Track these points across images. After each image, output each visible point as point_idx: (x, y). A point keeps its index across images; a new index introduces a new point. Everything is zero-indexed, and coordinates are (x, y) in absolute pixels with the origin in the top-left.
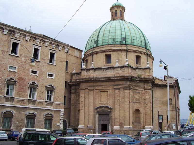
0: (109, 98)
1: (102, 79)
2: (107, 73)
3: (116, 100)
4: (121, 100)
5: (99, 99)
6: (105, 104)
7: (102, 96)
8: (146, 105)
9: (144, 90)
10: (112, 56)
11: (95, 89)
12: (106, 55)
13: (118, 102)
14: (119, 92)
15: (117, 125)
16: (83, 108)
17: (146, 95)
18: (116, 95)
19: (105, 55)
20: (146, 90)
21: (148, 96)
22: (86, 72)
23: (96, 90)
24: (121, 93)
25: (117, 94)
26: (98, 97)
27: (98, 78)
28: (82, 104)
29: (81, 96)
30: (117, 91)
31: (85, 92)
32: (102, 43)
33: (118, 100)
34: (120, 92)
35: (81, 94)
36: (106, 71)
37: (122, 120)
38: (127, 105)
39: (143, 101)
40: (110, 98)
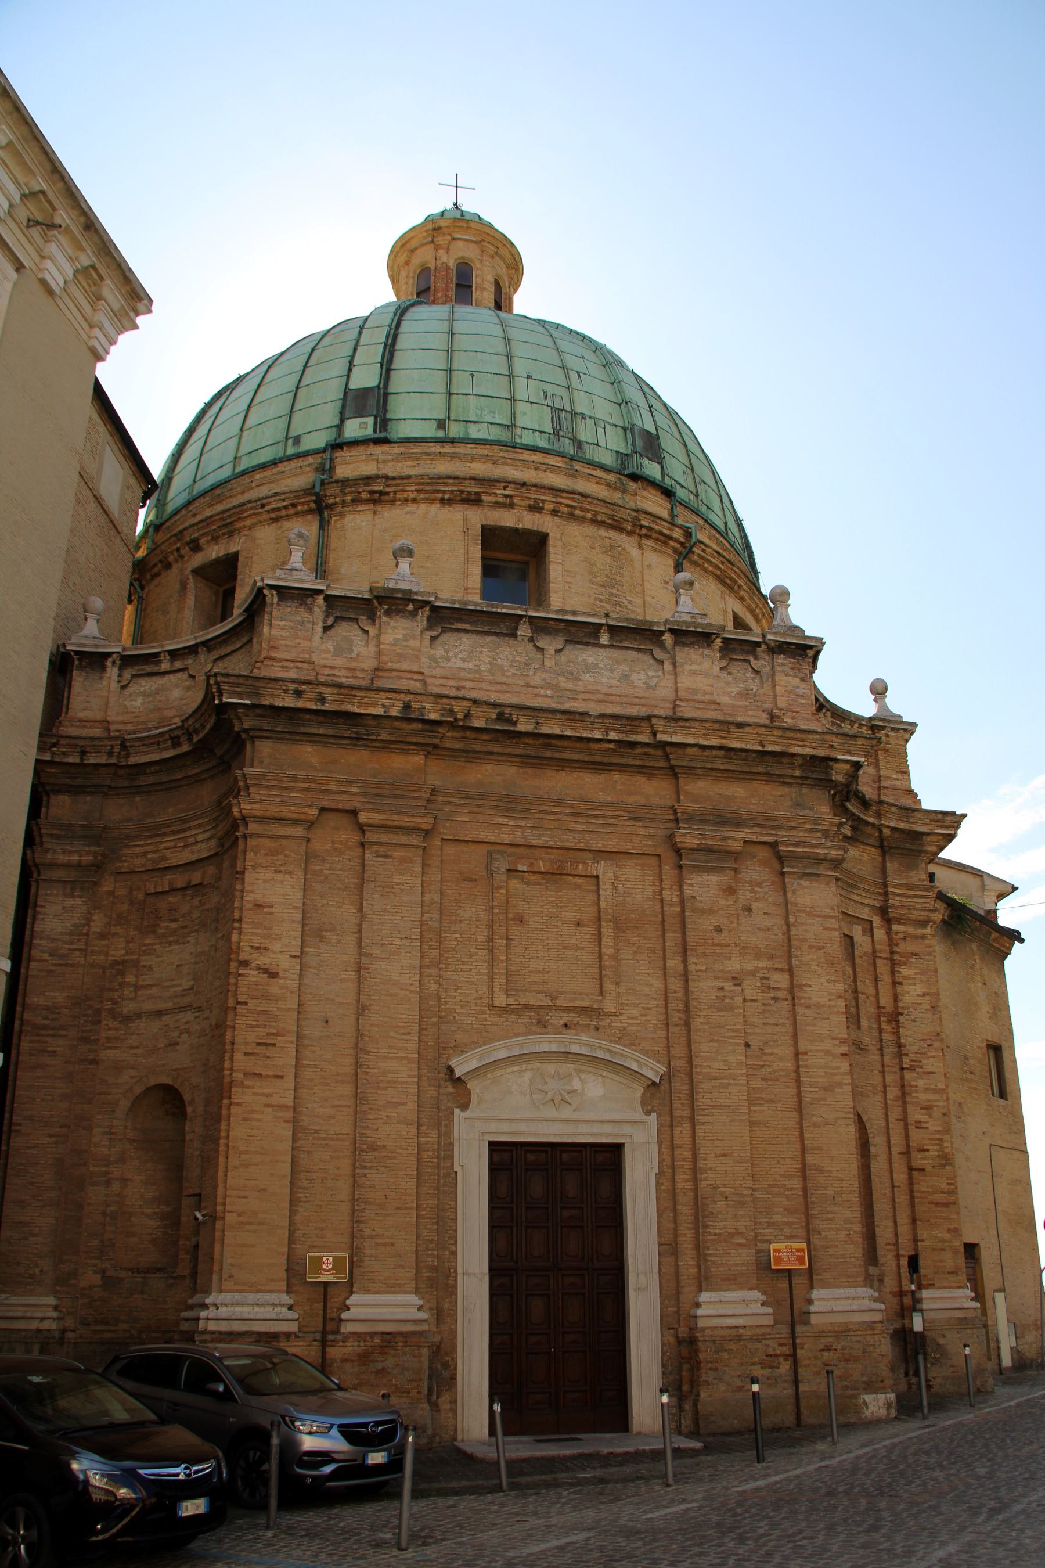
0: (615, 957)
1: (545, 730)
2: (587, 677)
3: (705, 989)
4: (751, 987)
5: (492, 961)
6: (565, 1018)
7: (521, 920)
8: (908, 1075)
9: (877, 921)
10: (554, 552)
11: (446, 830)
12: (490, 536)
13: (732, 1008)
14: (730, 891)
15: (732, 1281)
16: (284, 1058)
17: (904, 971)
18: (708, 923)
19: (483, 527)
20: (899, 921)
21: (919, 989)
22: (326, 629)
23: (450, 849)
24: (749, 910)
25: (711, 912)
26: (481, 938)
27: (504, 713)
28: (272, 1008)
29: (249, 897)
30: (713, 879)
31: (309, 857)
32: (442, 424)
33: (728, 986)
34: (744, 896)
35: (249, 876)
36: (563, 658)
37: (777, 1218)
38: (827, 1045)
39: (876, 1034)
40: (626, 953)
